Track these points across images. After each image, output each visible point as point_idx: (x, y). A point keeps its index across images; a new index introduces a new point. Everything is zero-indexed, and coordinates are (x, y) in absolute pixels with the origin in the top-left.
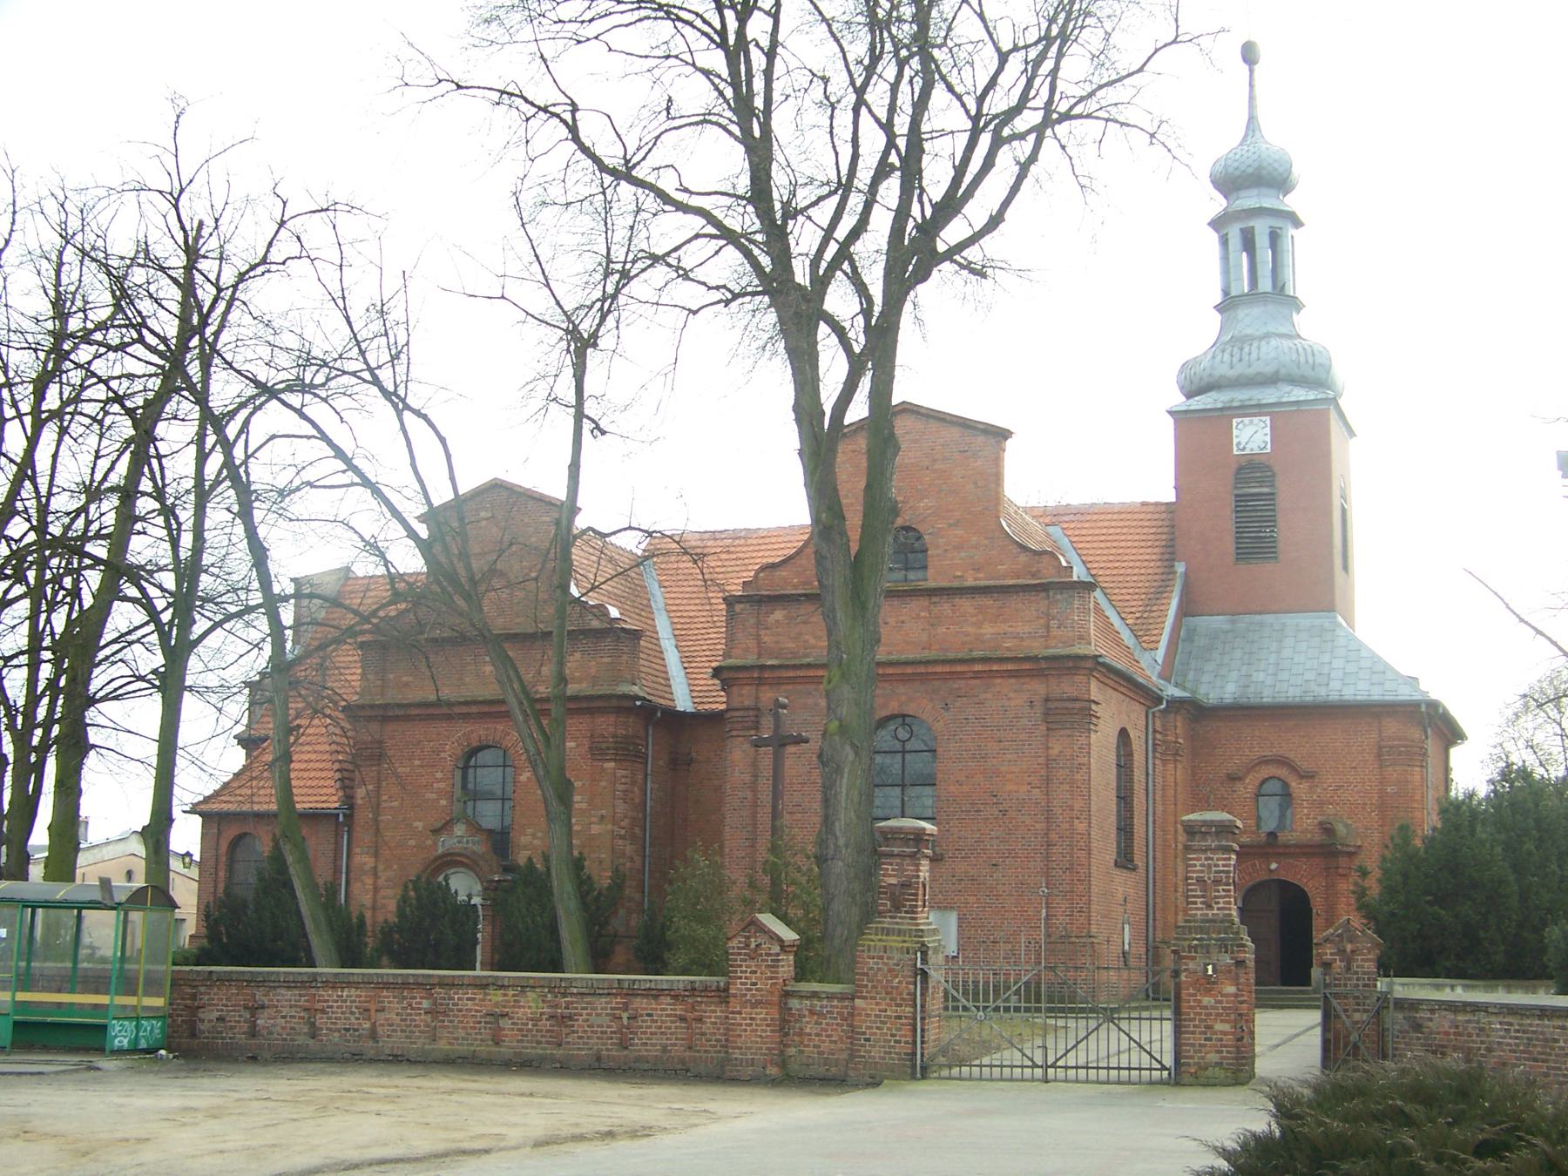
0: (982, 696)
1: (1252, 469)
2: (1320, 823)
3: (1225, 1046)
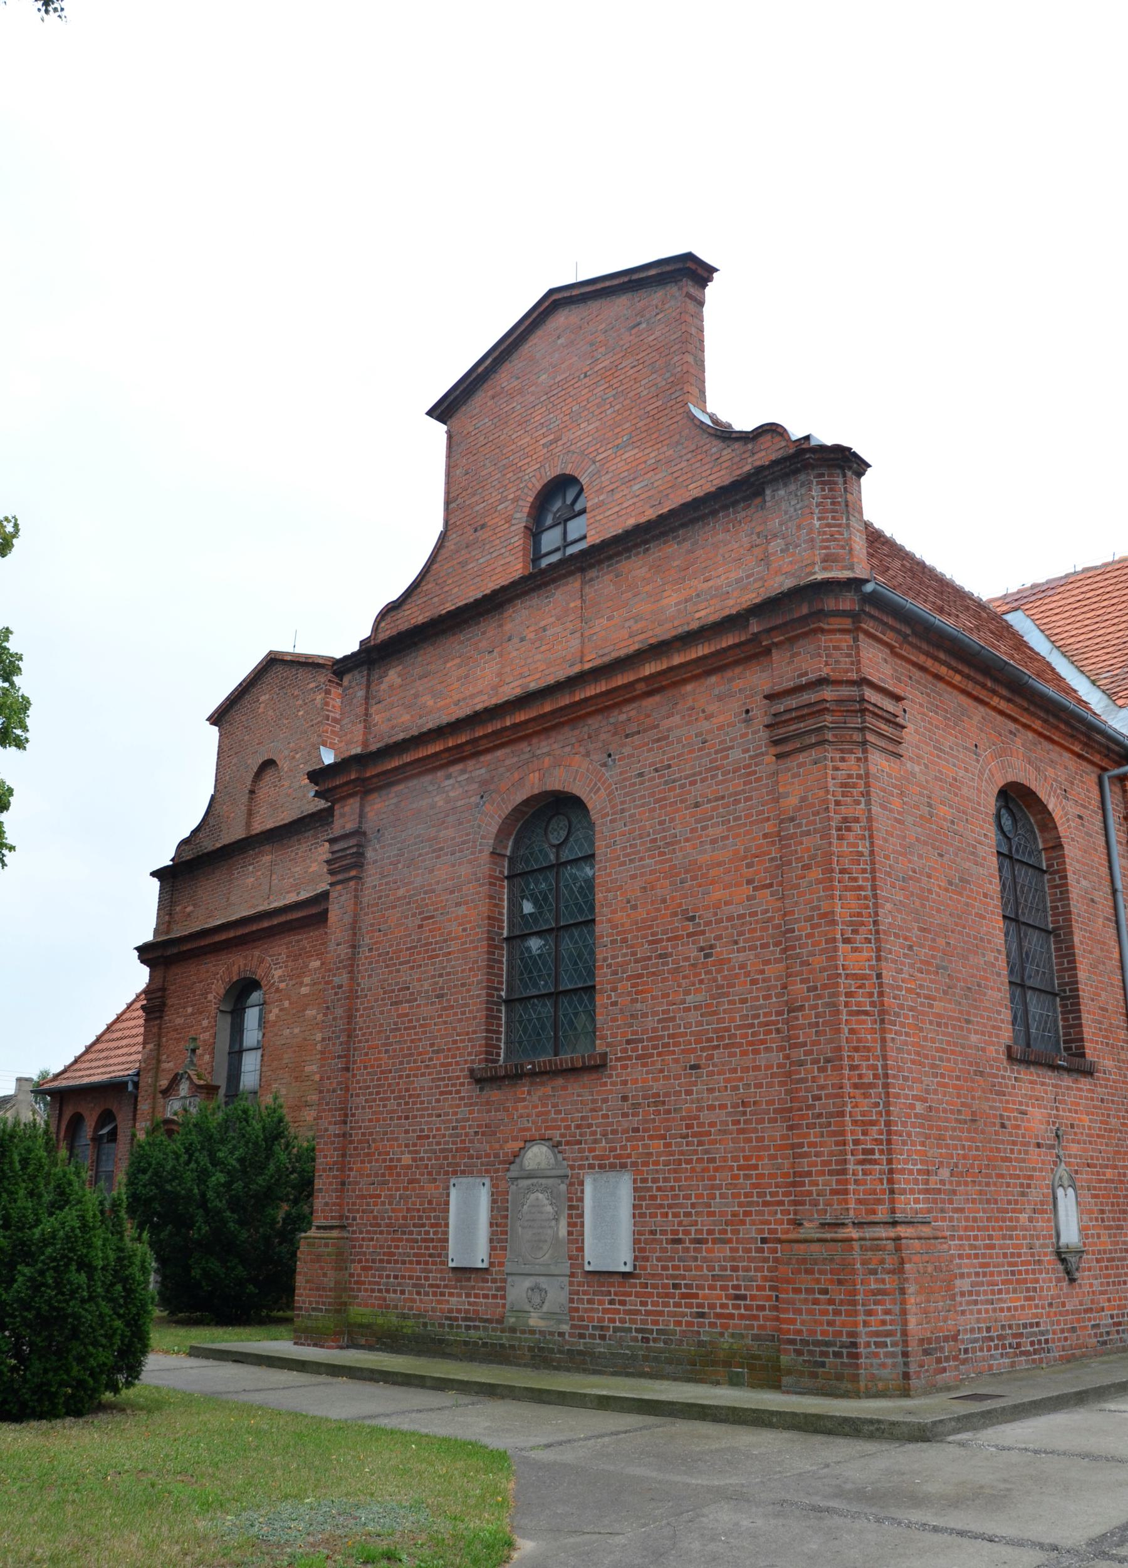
0: (666, 724)
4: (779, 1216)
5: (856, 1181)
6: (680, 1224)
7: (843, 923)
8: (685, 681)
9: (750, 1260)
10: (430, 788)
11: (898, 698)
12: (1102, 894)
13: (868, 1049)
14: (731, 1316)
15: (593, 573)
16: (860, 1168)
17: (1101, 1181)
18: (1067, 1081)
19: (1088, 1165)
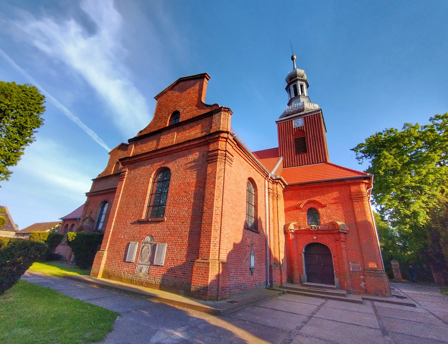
1: (300, 130)
2: (331, 222)
4: (195, 256)
5: (212, 250)
6: (175, 256)
7: (216, 196)
8: (193, 148)
9: (188, 265)
10: (142, 164)
11: (233, 156)
12: (263, 201)
13: (218, 222)
14: (182, 278)
15: (179, 127)
16: (213, 247)
17: (259, 255)
18: (254, 234)
19: (257, 251)
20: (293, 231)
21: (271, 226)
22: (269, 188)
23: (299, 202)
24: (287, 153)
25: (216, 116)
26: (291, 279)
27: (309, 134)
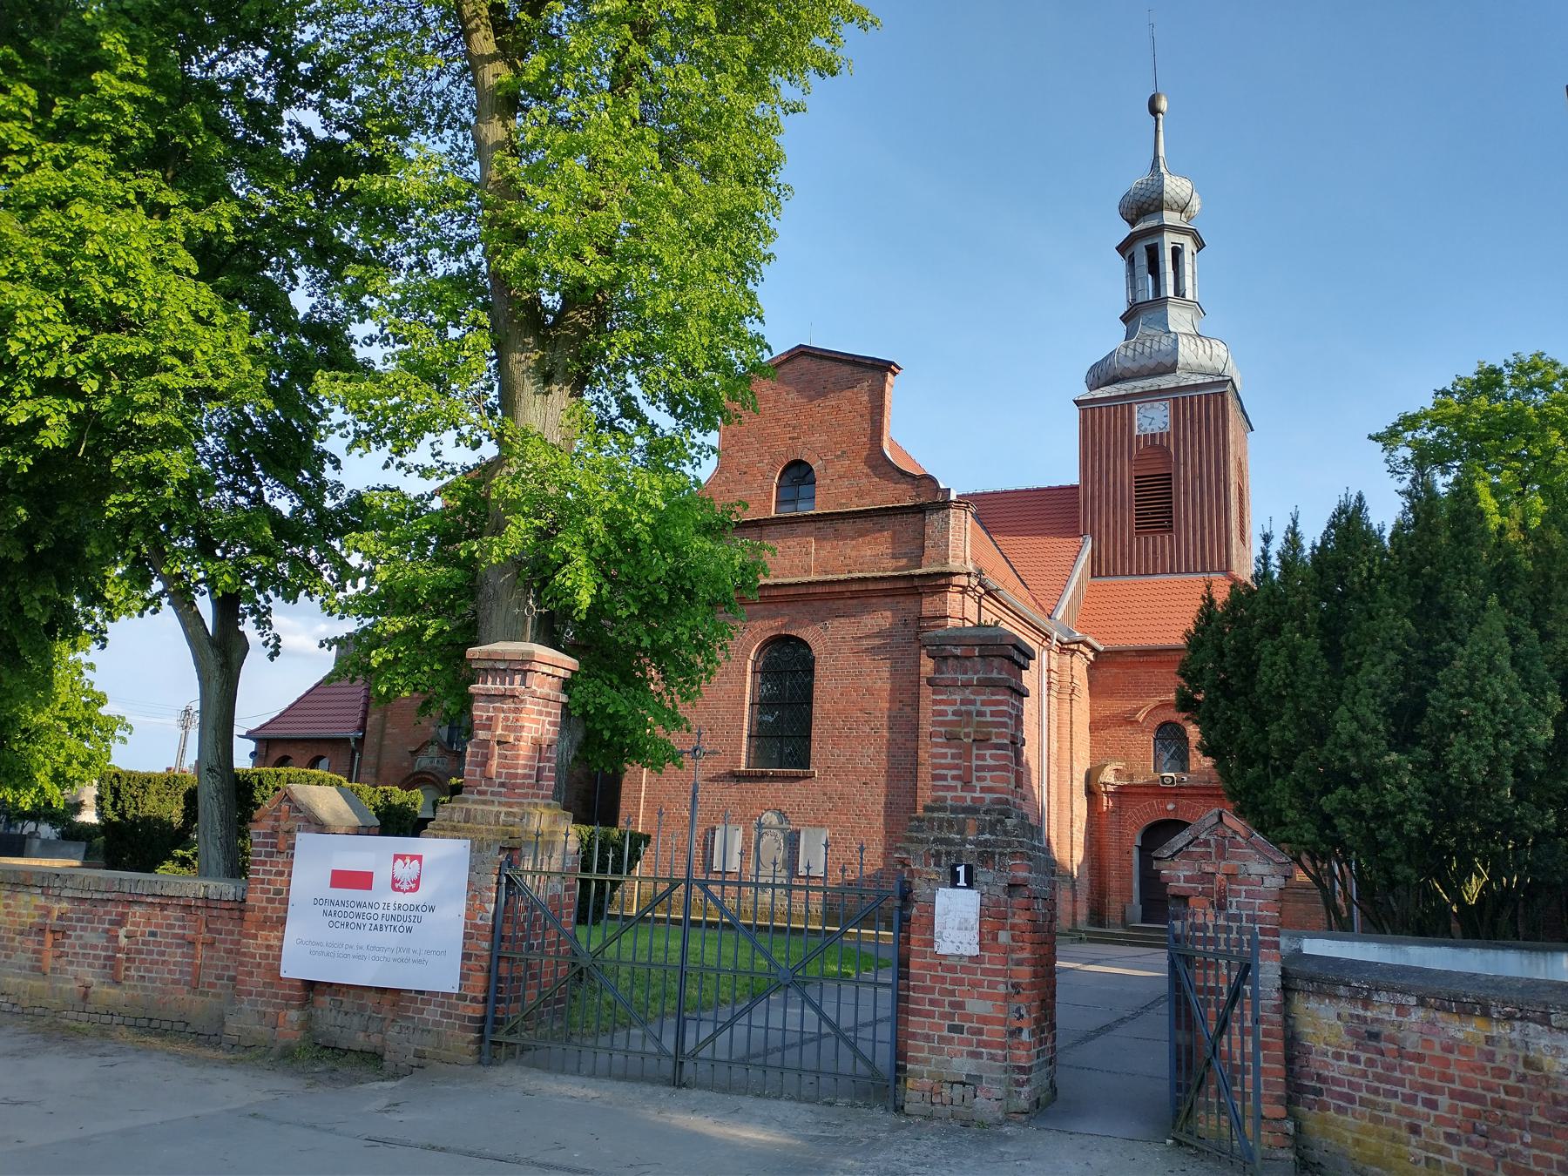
1: (1155, 444)
3: (987, 1044)
20: (1110, 788)
21: (1053, 777)
22: (1049, 670)
23: (1133, 705)
24: (1107, 525)
25: (934, 519)
26: (1098, 915)
27: (1185, 464)
